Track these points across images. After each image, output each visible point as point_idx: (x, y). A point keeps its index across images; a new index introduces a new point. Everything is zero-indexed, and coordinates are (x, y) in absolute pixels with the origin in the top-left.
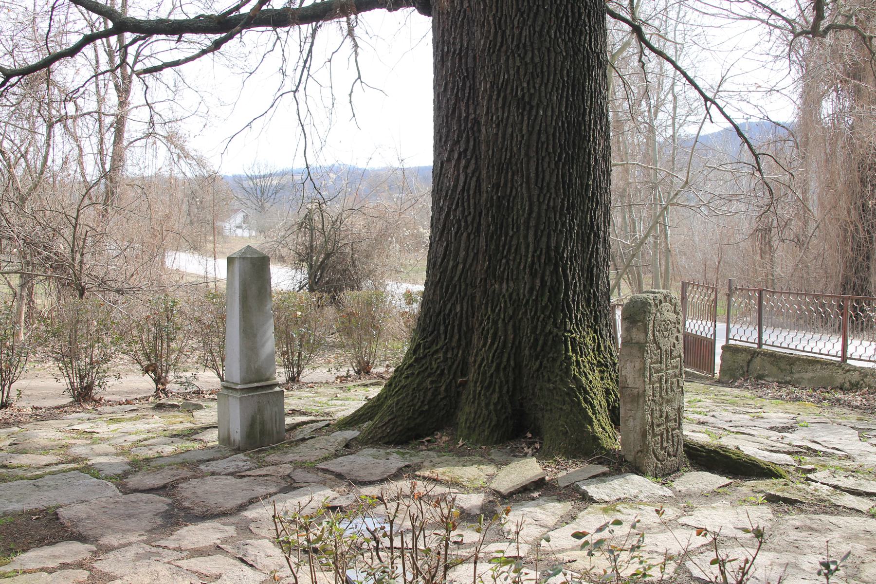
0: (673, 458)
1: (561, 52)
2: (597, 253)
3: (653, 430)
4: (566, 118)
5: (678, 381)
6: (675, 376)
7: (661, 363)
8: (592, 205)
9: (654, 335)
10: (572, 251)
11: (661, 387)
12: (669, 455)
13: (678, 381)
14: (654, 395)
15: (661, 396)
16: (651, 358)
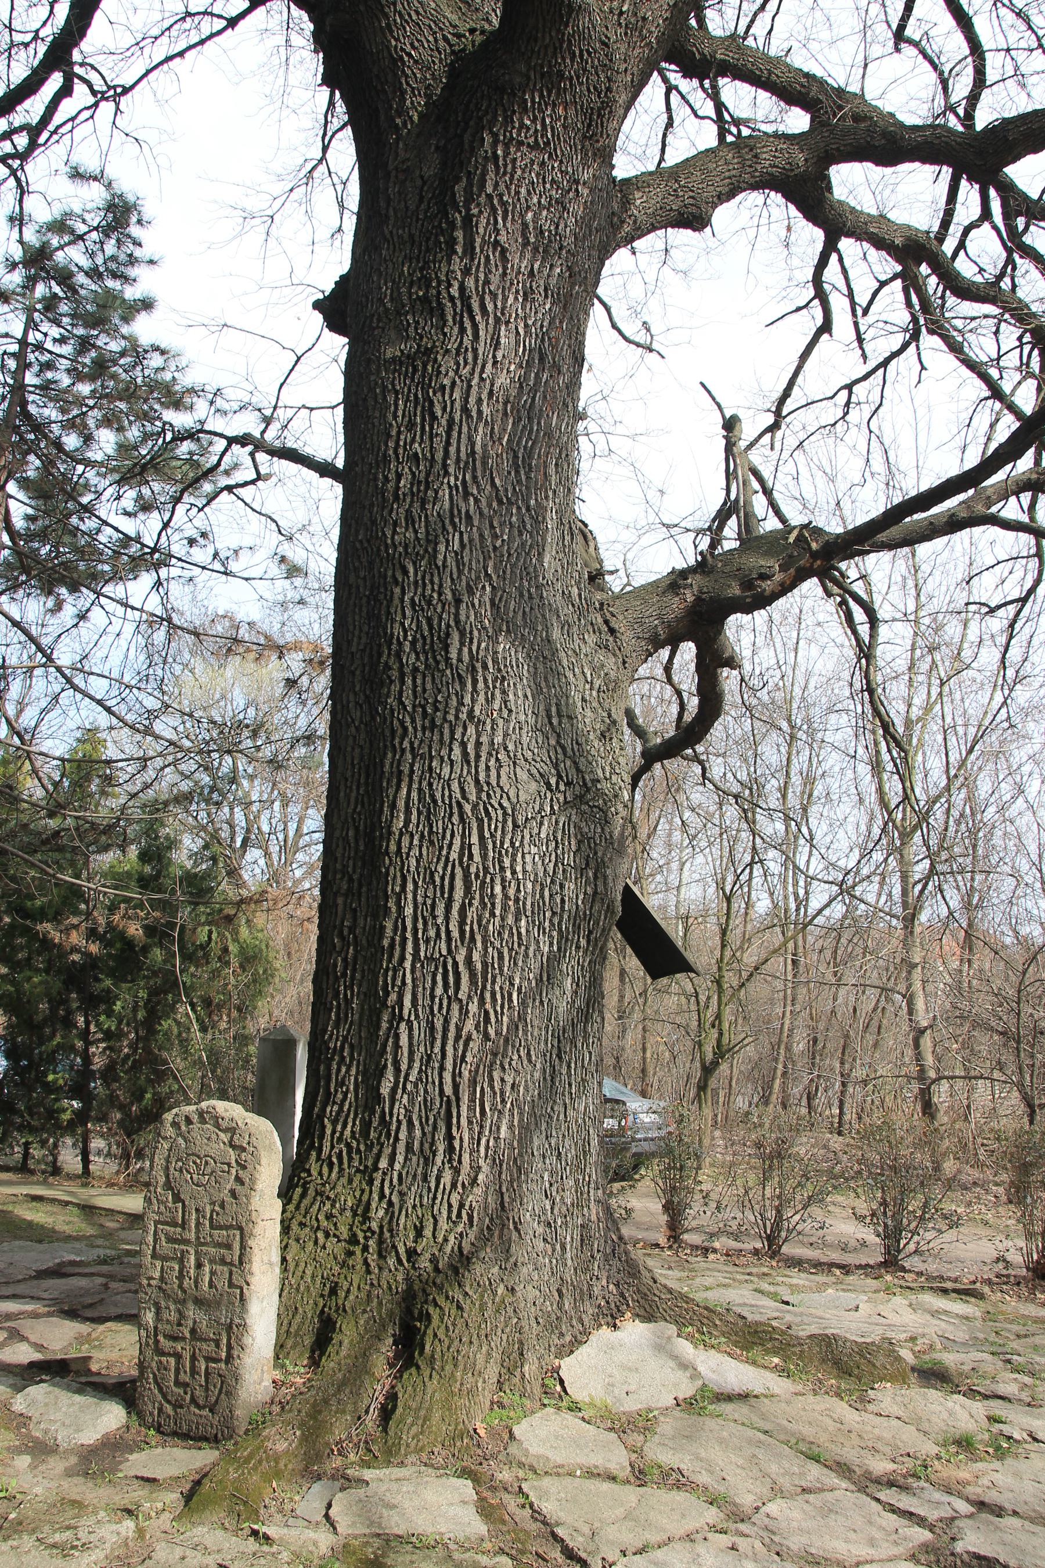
0: (205, 1412)
1: (353, 721)
2: (397, 1046)
3: (157, 1342)
4: (354, 819)
5: (231, 1274)
6: (223, 1262)
7: (184, 1228)
8: (389, 961)
9: (167, 1176)
10: (345, 1038)
11: (181, 1271)
12: (193, 1400)
13: (231, 1274)
14: (162, 1279)
15: (180, 1286)
16: (159, 1213)
